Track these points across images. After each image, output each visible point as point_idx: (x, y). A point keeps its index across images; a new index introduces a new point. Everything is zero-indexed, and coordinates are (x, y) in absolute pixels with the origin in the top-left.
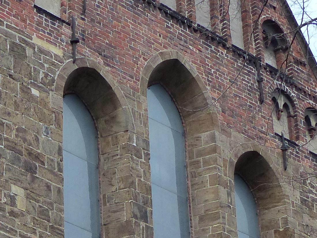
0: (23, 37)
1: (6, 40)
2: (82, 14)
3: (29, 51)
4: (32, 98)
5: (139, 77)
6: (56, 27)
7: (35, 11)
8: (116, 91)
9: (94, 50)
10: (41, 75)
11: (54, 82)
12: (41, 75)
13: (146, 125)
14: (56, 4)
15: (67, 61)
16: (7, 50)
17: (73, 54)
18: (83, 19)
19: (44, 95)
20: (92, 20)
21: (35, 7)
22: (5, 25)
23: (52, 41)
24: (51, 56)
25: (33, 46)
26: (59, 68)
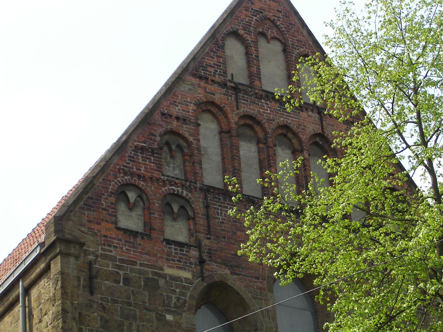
0: (155, 270)
1: (140, 278)
2: (207, 234)
3: (162, 282)
4: (167, 323)
5: (265, 277)
6: (184, 253)
7: (164, 244)
8: (245, 296)
9: (221, 263)
10: (174, 300)
11: (186, 304)
12: (174, 300)
13: (274, 319)
14: (184, 230)
15: (197, 281)
16: (141, 286)
17: (202, 273)
18: (209, 239)
19: (177, 317)
20: (217, 237)
21: (165, 240)
22: (138, 264)
23: (181, 266)
24: (182, 281)
25: (164, 276)
26: (189, 289)
